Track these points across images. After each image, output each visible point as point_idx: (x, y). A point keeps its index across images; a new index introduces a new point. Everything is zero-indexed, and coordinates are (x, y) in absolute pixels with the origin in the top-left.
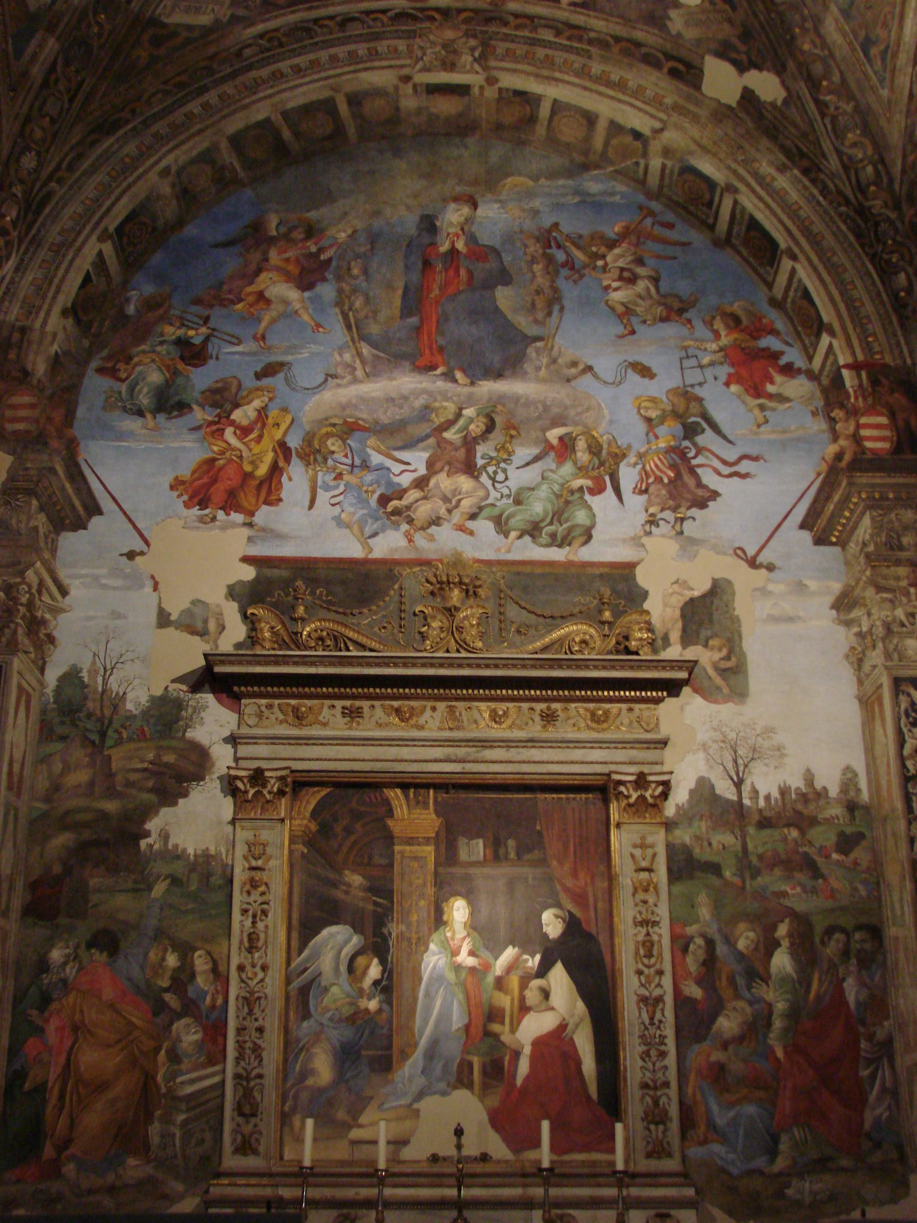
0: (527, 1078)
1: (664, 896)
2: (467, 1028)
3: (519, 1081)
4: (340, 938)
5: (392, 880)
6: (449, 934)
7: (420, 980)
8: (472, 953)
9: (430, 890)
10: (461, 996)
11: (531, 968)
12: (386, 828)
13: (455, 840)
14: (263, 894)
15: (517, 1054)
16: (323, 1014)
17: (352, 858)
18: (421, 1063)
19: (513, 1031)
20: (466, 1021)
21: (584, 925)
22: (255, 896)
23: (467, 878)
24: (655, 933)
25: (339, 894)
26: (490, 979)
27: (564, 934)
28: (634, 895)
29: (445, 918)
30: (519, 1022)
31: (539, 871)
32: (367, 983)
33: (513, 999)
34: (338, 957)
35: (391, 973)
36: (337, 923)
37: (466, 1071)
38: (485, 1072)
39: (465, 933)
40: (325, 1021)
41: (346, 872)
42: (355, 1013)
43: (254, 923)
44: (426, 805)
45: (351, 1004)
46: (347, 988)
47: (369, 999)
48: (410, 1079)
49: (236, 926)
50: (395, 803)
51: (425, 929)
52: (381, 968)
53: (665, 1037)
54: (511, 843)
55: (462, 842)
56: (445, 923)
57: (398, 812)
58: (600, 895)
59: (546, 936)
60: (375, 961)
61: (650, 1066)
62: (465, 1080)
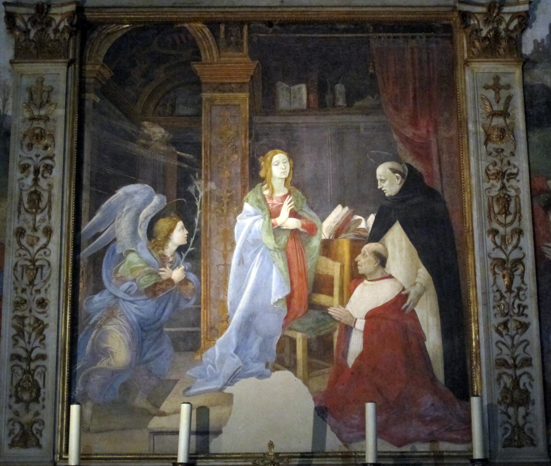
0: (361, 357)
1: (522, 146)
2: (289, 299)
3: (351, 361)
4: (138, 199)
5: (200, 133)
6: (266, 193)
7: (233, 244)
8: (293, 214)
9: (244, 142)
10: (281, 263)
11: (364, 230)
12: (193, 73)
13: (273, 85)
14: (46, 148)
15: (347, 329)
16: (118, 287)
17: (152, 106)
18: (234, 341)
19: (343, 302)
20: (288, 292)
21: (426, 181)
22: (38, 149)
23: (287, 129)
24: (512, 187)
25: (136, 149)
26: (316, 243)
27: (402, 191)
28: (486, 144)
29: (262, 174)
30: (351, 293)
31: (372, 119)
32: (171, 248)
33: (342, 267)
34: (135, 220)
35: (198, 237)
36: (133, 182)
37: (287, 350)
38: (310, 351)
39: (286, 191)
40: (120, 294)
41: (146, 123)
42: (155, 285)
43: (36, 180)
44: (238, 46)
45: (151, 274)
46: (147, 255)
47: (173, 268)
48: (222, 361)
49: (14, 186)
50: (202, 45)
51: (239, 186)
52: (186, 232)
53: (525, 307)
54: (340, 88)
55: (281, 88)
56: (262, 180)
57: (205, 56)
58: (444, 146)
59: (381, 192)
60: (180, 224)
61: (509, 342)
62: (287, 361)
